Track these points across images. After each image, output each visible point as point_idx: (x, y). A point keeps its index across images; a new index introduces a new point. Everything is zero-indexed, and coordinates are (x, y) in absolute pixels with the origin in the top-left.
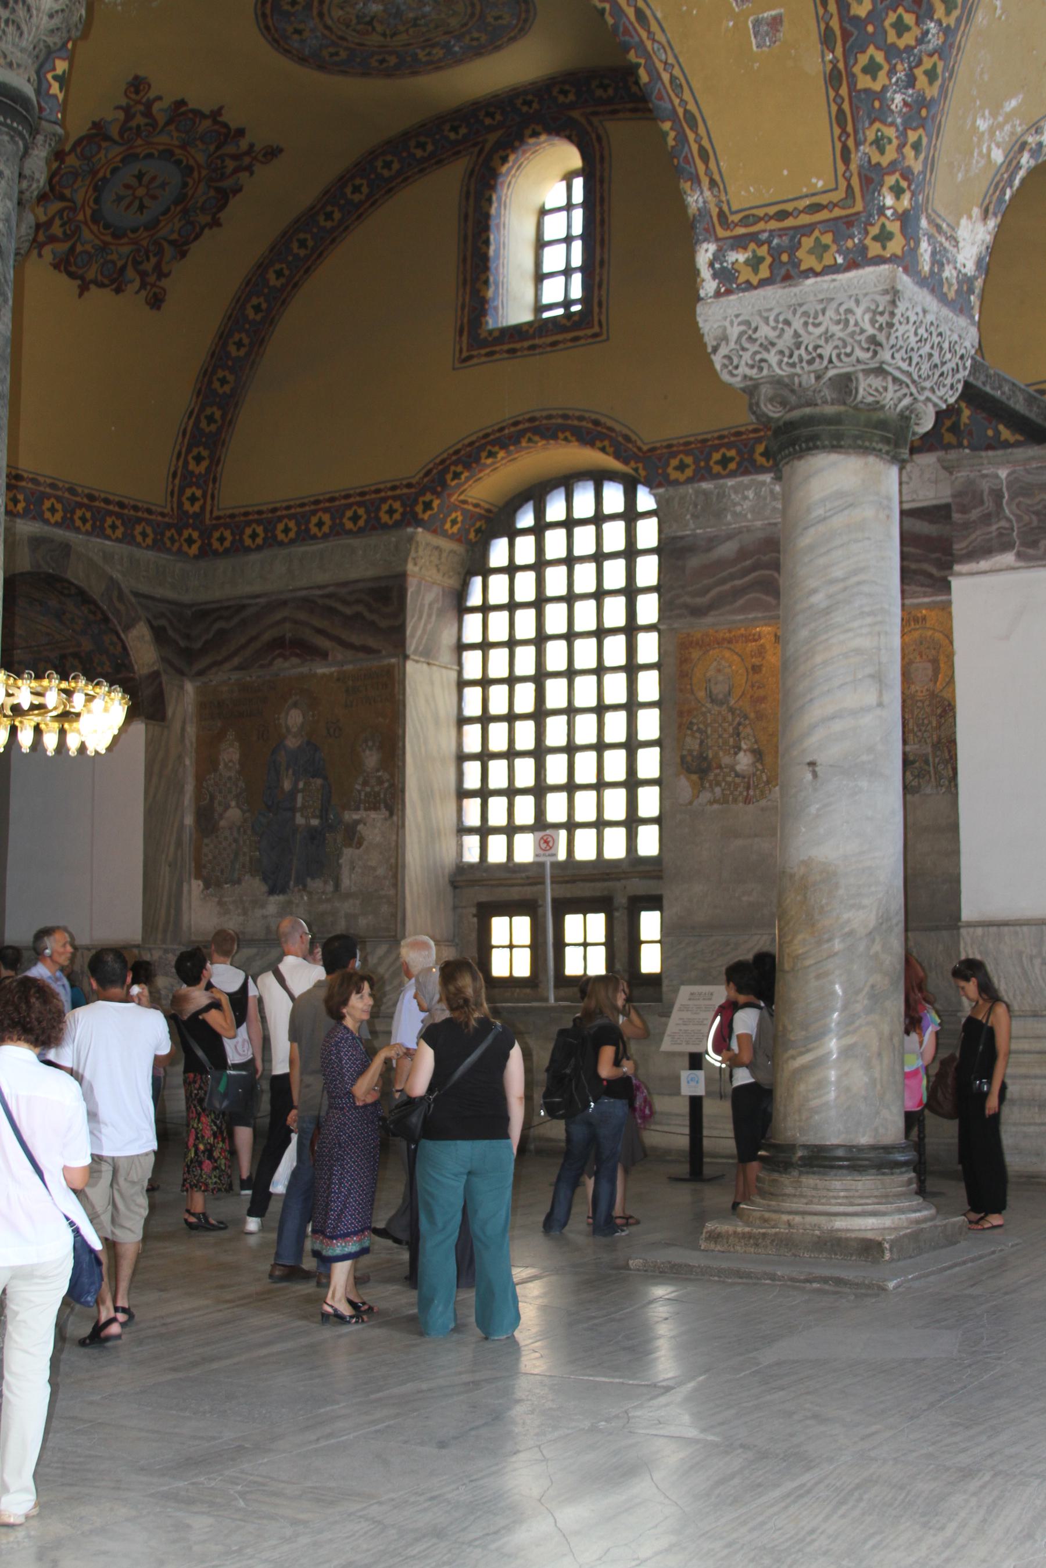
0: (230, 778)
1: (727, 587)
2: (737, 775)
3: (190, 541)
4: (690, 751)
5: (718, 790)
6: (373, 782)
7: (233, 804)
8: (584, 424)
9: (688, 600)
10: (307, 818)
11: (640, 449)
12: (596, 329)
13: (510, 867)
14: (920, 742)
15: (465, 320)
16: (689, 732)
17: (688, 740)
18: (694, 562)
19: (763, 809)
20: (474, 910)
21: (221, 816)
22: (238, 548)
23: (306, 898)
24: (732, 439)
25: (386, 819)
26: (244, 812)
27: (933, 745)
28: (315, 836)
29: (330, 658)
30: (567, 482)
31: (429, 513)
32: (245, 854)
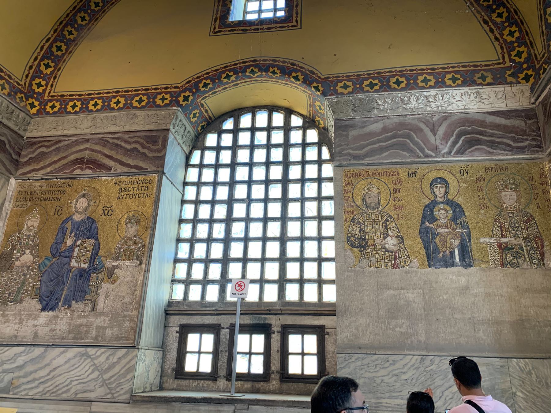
0: (29, 236)
1: (376, 146)
2: (387, 251)
3: (32, 106)
4: (353, 235)
5: (373, 259)
6: (130, 243)
7: (28, 252)
8: (286, 64)
9: (351, 151)
10: (80, 263)
11: (320, 77)
12: (295, 23)
13: (202, 302)
14: (515, 236)
15: (218, 16)
16: (352, 223)
17: (352, 228)
18: (353, 133)
19: (406, 272)
20: (178, 329)
21: (17, 259)
22: (63, 111)
23: (69, 314)
24: (376, 75)
25: (136, 267)
26: (34, 257)
27: (524, 239)
28: (83, 274)
29: (112, 171)
30: (253, 110)
31: (186, 102)
32: (29, 284)
